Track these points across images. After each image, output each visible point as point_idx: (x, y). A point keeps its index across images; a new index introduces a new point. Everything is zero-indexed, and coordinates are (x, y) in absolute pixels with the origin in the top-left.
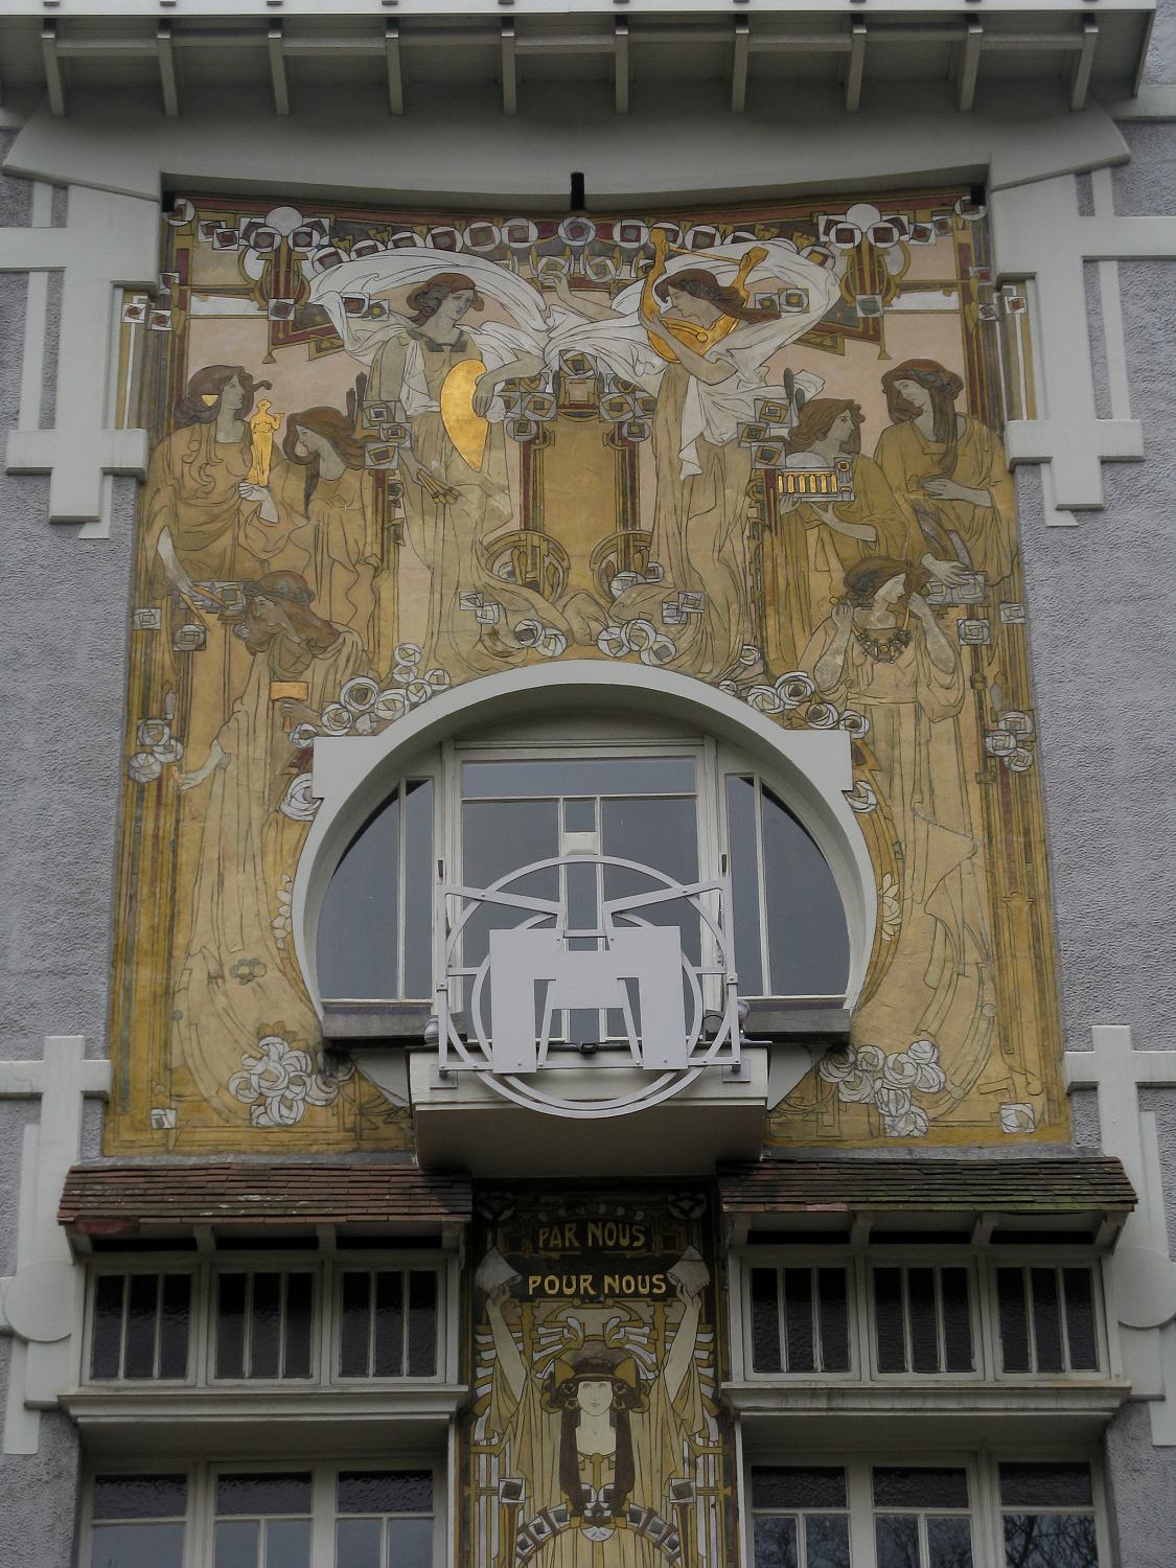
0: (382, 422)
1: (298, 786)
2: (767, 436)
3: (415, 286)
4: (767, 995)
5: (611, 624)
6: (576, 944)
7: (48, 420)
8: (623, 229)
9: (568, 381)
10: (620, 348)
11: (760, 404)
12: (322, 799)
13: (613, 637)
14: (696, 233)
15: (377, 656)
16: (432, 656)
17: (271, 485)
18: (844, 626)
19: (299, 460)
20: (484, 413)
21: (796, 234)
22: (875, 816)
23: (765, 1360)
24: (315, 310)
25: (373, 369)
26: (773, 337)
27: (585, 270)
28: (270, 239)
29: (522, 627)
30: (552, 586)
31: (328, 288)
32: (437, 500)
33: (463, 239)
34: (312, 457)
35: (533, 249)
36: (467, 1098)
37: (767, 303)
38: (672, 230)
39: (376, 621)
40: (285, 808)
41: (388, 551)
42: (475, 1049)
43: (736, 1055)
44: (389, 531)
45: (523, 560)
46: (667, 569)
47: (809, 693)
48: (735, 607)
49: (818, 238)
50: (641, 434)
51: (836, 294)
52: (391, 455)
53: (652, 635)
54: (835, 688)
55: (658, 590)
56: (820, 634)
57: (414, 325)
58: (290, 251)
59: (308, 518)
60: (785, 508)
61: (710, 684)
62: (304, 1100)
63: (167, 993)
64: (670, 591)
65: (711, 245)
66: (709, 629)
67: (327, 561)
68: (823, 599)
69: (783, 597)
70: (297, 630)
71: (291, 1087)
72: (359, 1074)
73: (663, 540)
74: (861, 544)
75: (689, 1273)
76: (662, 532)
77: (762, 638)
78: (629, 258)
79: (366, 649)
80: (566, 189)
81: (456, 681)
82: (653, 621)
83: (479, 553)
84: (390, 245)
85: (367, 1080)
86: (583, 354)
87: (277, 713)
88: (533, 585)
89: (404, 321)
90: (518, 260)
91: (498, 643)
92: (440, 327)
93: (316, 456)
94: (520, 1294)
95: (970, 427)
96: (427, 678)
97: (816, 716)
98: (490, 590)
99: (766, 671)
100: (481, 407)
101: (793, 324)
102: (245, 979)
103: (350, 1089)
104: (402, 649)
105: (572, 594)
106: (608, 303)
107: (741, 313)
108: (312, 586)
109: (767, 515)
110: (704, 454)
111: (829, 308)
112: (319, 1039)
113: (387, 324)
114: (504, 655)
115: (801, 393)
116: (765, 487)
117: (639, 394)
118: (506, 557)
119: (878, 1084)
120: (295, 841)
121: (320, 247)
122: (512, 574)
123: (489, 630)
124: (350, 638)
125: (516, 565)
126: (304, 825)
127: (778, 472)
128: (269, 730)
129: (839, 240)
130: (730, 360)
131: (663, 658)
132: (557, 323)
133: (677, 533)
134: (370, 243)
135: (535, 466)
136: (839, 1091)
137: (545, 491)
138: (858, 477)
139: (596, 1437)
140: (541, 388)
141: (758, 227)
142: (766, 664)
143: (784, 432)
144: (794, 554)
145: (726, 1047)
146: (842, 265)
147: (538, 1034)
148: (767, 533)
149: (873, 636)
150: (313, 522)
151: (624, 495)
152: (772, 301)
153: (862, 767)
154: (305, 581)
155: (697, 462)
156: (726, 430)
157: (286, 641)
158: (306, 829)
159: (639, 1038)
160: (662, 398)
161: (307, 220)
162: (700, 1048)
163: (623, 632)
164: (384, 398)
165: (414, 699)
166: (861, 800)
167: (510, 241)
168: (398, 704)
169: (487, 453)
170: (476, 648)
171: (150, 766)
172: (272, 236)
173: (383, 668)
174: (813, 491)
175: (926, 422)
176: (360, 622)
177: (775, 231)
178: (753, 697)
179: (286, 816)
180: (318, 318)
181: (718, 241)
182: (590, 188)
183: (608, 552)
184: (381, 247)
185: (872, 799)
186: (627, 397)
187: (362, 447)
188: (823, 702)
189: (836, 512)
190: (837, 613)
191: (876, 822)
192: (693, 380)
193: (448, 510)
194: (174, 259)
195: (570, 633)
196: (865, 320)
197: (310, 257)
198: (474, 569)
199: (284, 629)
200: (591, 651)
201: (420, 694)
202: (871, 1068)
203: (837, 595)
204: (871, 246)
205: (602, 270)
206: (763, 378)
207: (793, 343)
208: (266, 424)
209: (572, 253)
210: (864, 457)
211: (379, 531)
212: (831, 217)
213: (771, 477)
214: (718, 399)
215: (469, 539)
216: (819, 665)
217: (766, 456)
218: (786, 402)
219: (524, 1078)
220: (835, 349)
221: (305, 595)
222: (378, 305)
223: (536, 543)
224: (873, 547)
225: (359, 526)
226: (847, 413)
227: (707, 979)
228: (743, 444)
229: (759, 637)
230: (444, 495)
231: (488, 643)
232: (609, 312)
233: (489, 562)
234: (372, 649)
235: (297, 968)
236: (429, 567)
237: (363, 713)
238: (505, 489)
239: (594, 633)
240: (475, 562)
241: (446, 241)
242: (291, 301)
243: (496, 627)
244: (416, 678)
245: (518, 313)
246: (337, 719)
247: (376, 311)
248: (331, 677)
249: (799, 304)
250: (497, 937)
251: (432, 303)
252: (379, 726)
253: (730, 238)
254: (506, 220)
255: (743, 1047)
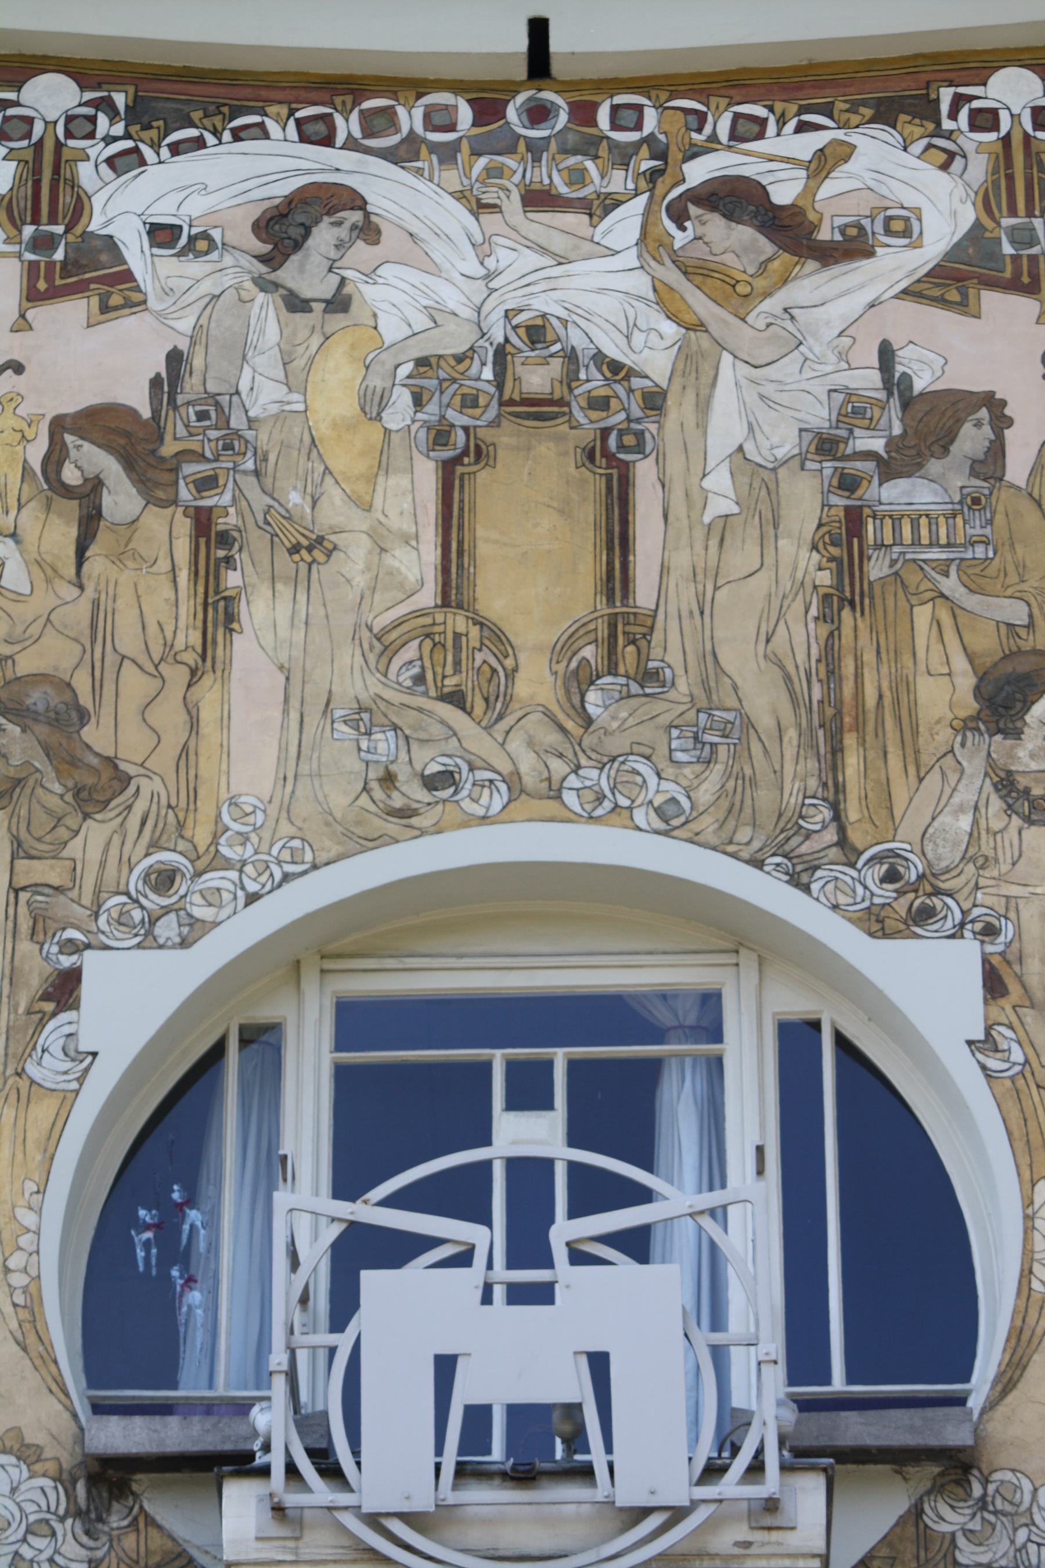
0: (208, 428)
1: (53, 1034)
2: (849, 451)
3: (267, 204)
4: (838, 1383)
5: (584, 761)
6: (519, 1295)
8: (615, 109)
9: (518, 361)
10: (608, 306)
11: (839, 398)
12: (94, 1054)
13: (588, 783)
14: (737, 116)
15: (191, 815)
16: (284, 814)
17: (19, 531)
18: (974, 765)
19: (67, 491)
20: (379, 414)
21: (903, 118)
22: (1021, 1082)
24: (98, 243)
25: (193, 343)
26: (862, 286)
27: (550, 177)
28: (26, 127)
29: (433, 768)
30: (486, 700)
32: (296, 557)
33: (348, 125)
34: (90, 486)
35: (465, 146)
37: (853, 232)
38: (695, 112)
39: (192, 757)
40: (32, 1069)
41: (215, 642)
42: (331, 1472)
43: (772, 1481)
44: (216, 610)
45: (438, 657)
46: (680, 671)
47: (913, 877)
48: (792, 734)
49: (938, 124)
50: (639, 448)
51: (968, 216)
52: (221, 482)
53: (652, 780)
54: (958, 870)
55: (665, 706)
56: (933, 779)
57: (263, 269)
58: (59, 146)
59: (81, 587)
60: (877, 569)
61: (747, 862)
62: (51, 1560)
64: (684, 707)
65: (760, 136)
66: (748, 772)
67: (111, 658)
68: (938, 722)
69: (871, 717)
70: (57, 771)
71: (30, 1538)
72: (147, 1515)
73: (673, 625)
74: (1003, 629)
76: (672, 610)
77: (836, 785)
78: (623, 156)
79: (173, 803)
80: (520, 43)
81: (323, 857)
82: (654, 758)
83: (366, 646)
84: (227, 136)
85: (159, 1527)
86: (544, 316)
87: (23, 909)
88: (456, 699)
89: (247, 262)
90: (441, 162)
91: (395, 794)
93: (95, 485)
96: (275, 851)
97: (924, 916)
98: (382, 705)
99: (843, 842)
103: (129, 1542)
104: (233, 803)
105: (520, 713)
106: (587, 232)
107: (809, 248)
108: (85, 700)
109: (847, 581)
110: (746, 480)
111: (955, 239)
112: (80, 1458)
113: (219, 266)
114: (405, 813)
115: (906, 378)
117: (636, 383)
118: (410, 652)
119: (1022, 1535)
120: (47, 1125)
121: (109, 140)
122: (420, 679)
123: (381, 773)
124: (147, 786)
125: (427, 664)
126: (65, 1098)
127: (867, 511)
128: (9, 939)
129: (974, 127)
130: (788, 325)
132: (502, 265)
133: (697, 613)
134: (192, 133)
135: (462, 501)
136: (956, 1547)
137: (480, 544)
138: (999, 519)
140: (474, 371)
141: (840, 106)
142: (842, 830)
143: (878, 445)
144: (892, 646)
145: (756, 1469)
146: (978, 169)
147: (439, 1450)
148: (846, 613)
149: (1022, 782)
150: (90, 592)
151: (610, 549)
152: (861, 228)
153: (1002, 1002)
154: (74, 691)
155: (734, 497)
157: (39, 791)
158: (68, 1103)
159: (610, 1458)
160: (676, 387)
161: (89, 96)
162: (713, 1471)
163: (604, 776)
164: (212, 388)
165: (252, 887)
166: (999, 1055)
167: (426, 129)
168: (227, 897)
169: (381, 479)
170: (359, 803)
172: (29, 121)
173: (202, 837)
174: (925, 541)
176: (165, 760)
177: (868, 112)
178: (821, 883)
179: (32, 1082)
180: (104, 258)
181: (771, 128)
182: (558, 43)
183: (581, 642)
184: (210, 139)
185: (1017, 1056)
186: (620, 390)
187: (176, 470)
188: (937, 892)
189: (964, 578)
190: (963, 745)
192: (727, 358)
193: (314, 575)
195: (515, 778)
196: (1016, 259)
197: (93, 157)
198: (357, 675)
199: (38, 770)
200: (551, 807)
201: (264, 878)
202: (1008, 1508)
203: (963, 714)
204: (1027, 136)
205: (578, 177)
206: (843, 356)
207: (896, 297)
209: (529, 149)
210: (1012, 486)
211: (200, 609)
212: (962, 90)
213: (854, 519)
214: (769, 390)
215: (350, 619)
216: (931, 830)
217: (848, 484)
218: (882, 395)
220: (964, 306)
221: (74, 715)
222: (205, 236)
223: (461, 628)
224: (1023, 633)
225: (166, 600)
226: (984, 413)
227: (737, 1355)
228: (809, 465)
229: (830, 783)
230: (310, 549)
231: (378, 793)
232: (587, 246)
233: (384, 660)
234: (183, 804)
235: (46, 1342)
236: (281, 668)
237: (167, 910)
238: (410, 540)
239: (556, 778)
240: (359, 660)
241: (321, 128)
242: (59, 229)
243: (393, 768)
244: (256, 853)
245: (439, 251)
246: (122, 921)
247: (202, 245)
248: (114, 852)
249: (906, 233)
250: (371, 1280)
251: (295, 232)
253: (792, 125)
254: (419, 96)
255: (785, 1468)
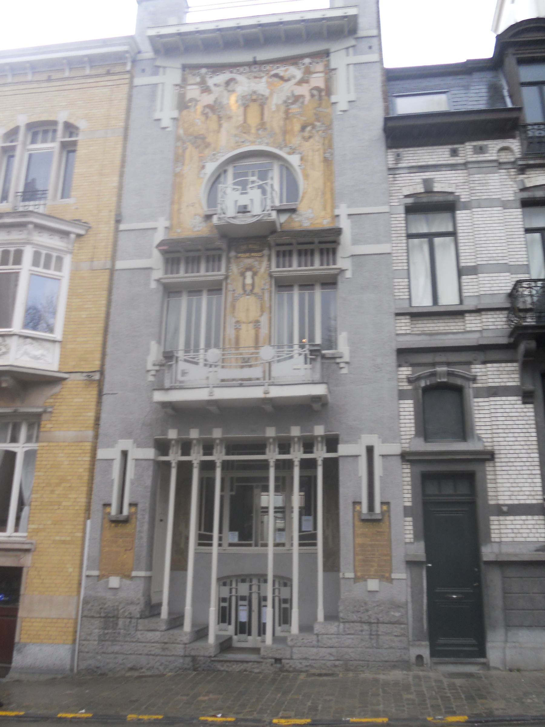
1: (203, 171)
7: (161, 110)
23: (278, 266)
31: (211, 82)
33: (235, 71)
36: (222, 222)
42: (224, 213)
60: (290, 115)
63: (179, 210)
75: (266, 252)
78: (264, 72)
88: (245, 133)
92: (230, 88)
94: (237, 258)
95: (325, 98)
100: (237, 101)
101: (294, 81)
102: (193, 206)
114: (239, 146)
116: (287, 112)
131: (267, 144)
139: (249, 281)
146: (303, 70)
156: (280, 102)
162: (264, 211)
171: (178, 170)
175: (317, 97)
191: (304, 170)
194: (184, 80)
208: (199, 108)
219: (233, 218)
220: (300, 85)
252: (217, 159)
